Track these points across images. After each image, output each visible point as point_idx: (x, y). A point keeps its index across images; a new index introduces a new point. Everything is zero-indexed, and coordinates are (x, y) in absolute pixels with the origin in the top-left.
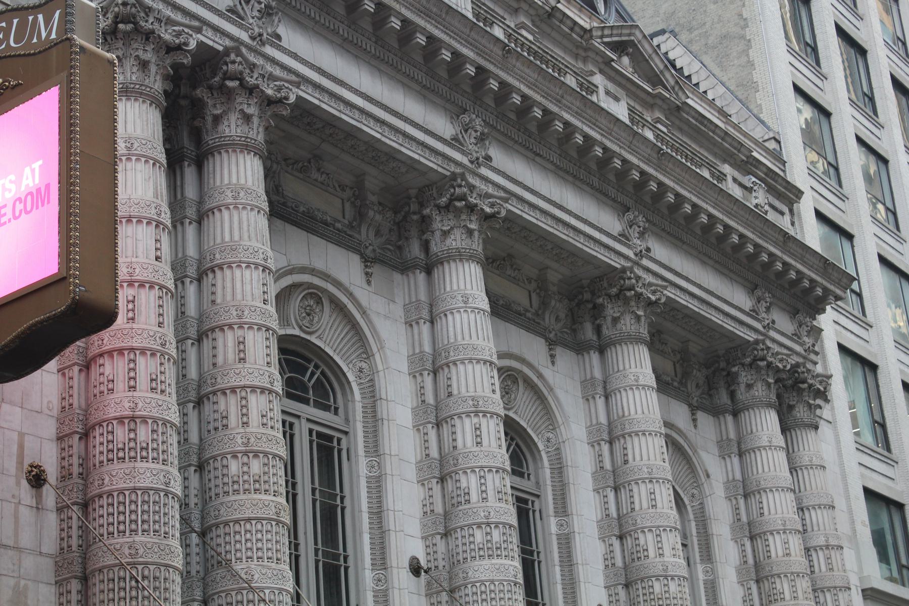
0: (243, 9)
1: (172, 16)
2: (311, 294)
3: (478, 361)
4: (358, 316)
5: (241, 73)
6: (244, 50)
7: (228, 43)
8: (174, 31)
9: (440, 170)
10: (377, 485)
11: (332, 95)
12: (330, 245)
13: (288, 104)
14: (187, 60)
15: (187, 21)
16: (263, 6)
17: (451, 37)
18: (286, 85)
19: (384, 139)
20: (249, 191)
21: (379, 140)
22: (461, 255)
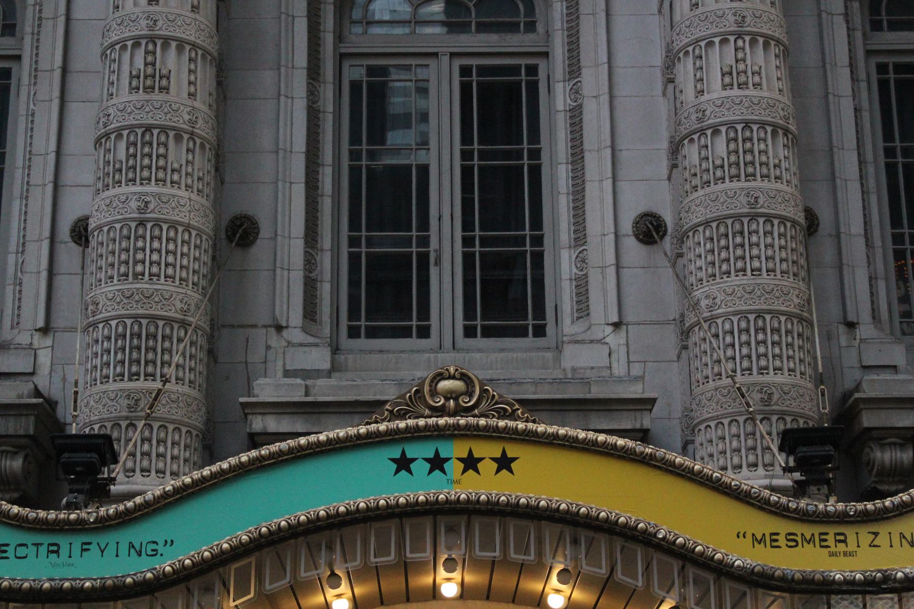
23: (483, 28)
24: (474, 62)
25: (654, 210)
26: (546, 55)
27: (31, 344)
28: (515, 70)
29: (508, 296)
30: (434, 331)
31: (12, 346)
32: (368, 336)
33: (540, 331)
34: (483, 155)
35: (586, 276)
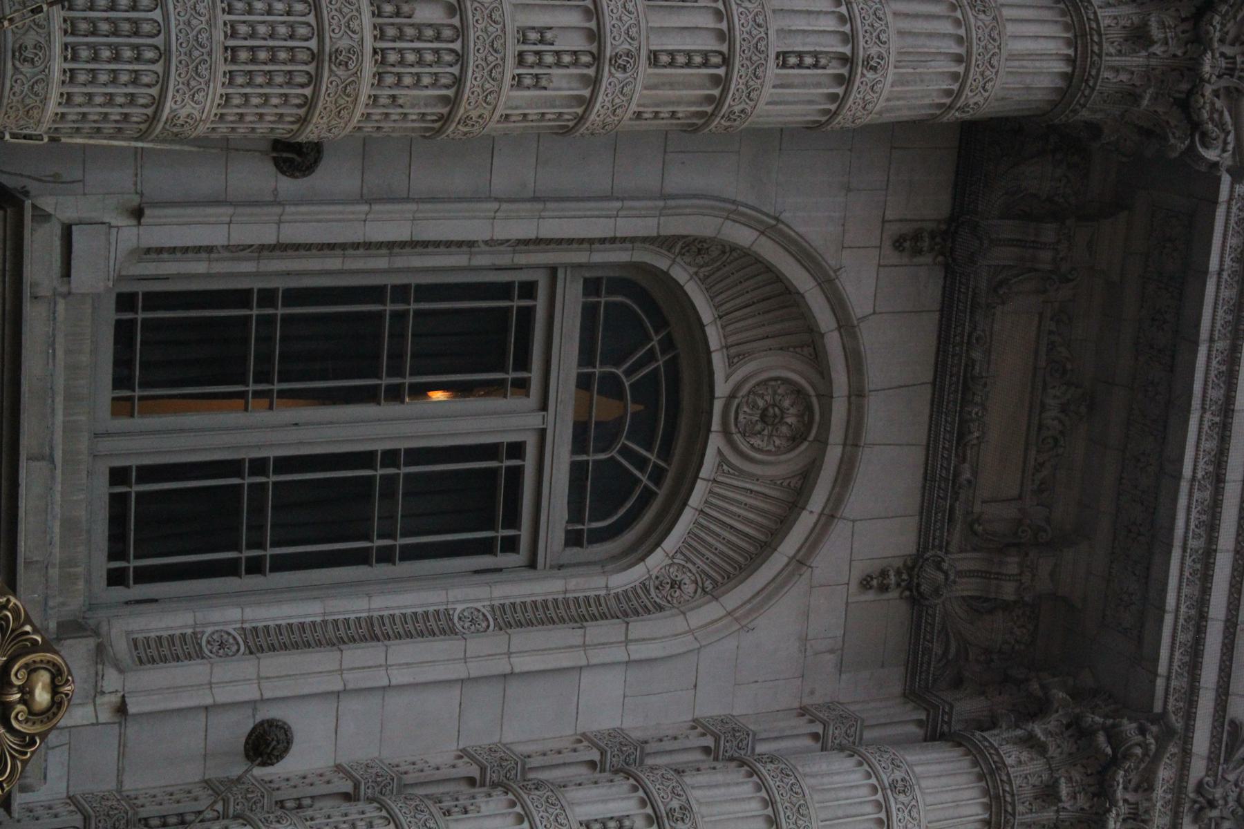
2: (809, 408)
6: (1172, 749)
7: (1178, 724)
8: (1221, 113)
9: (1160, 682)
10: (434, 626)
14: (1178, 145)
19: (1184, 486)
20: (995, 34)
21: (1178, 477)
22: (992, 773)
23: (578, 472)
24: (540, 303)
25: (294, 748)
26: (532, 565)
27: (103, 693)
28: (523, 362)
29: (179, 528)
30: (123, 423)
31: (100, 667)
32: (119, 324)
33: (116, 578)
34: (399, 317)
35: (201, 655)
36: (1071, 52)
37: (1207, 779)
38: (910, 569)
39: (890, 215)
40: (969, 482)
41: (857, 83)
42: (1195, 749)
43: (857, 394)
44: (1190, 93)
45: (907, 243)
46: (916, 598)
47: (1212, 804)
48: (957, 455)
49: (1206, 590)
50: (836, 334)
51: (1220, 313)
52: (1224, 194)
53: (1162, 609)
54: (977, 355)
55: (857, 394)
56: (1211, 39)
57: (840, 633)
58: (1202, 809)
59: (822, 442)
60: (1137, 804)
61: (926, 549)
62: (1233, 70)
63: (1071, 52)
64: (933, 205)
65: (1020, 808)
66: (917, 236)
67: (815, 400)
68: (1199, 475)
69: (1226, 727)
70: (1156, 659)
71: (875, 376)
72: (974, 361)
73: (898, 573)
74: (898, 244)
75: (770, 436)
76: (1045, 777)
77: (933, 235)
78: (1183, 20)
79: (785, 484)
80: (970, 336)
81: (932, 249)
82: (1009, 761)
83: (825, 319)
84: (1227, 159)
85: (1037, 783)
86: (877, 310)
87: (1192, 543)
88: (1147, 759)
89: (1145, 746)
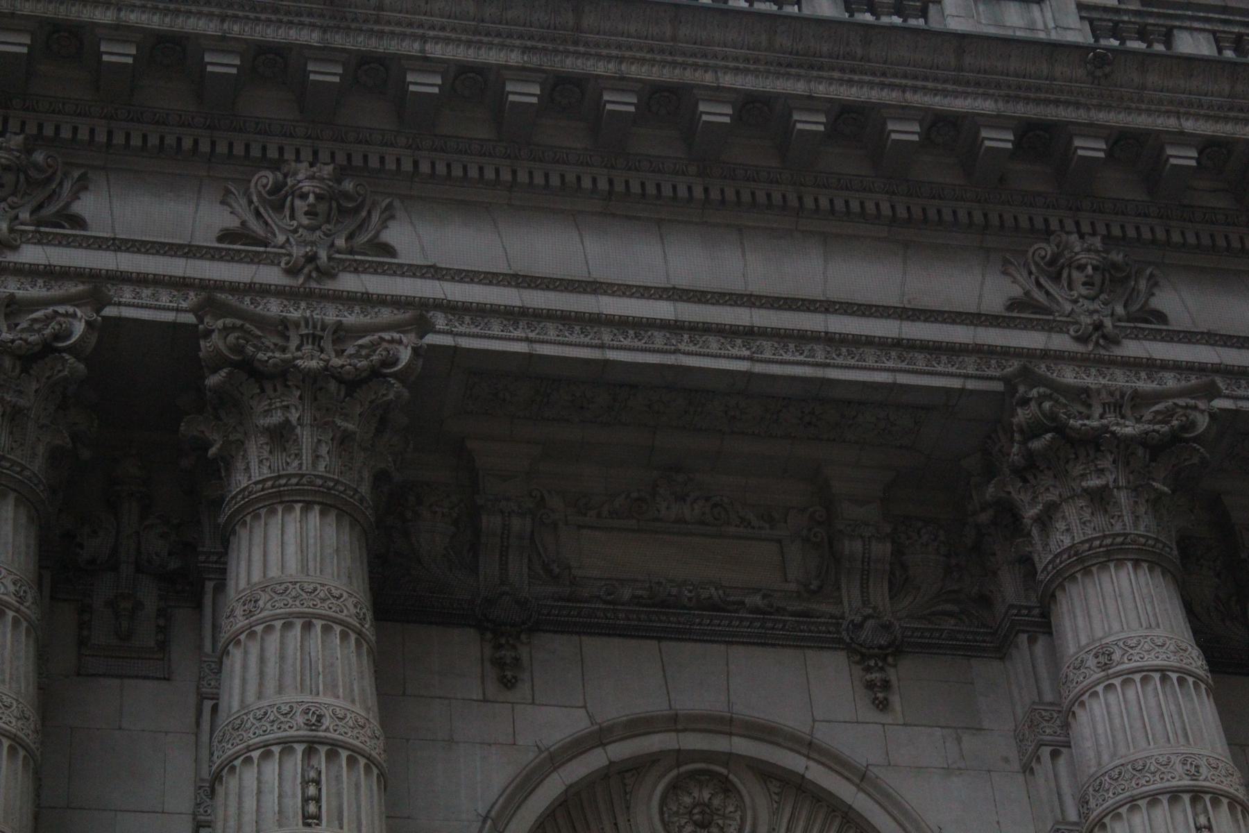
0: (1048, 293)
1: (20, 293)
2: (692, 775)
3: (1153, 799)
4: (845, 791)
5: (1053, 417)
6: (1042, 369)
7: (1014, 366)
8: (361, 346)
9: (971, 385)
11: (566, 319)
12: (739, 653)
13: (1196, 439)
15: (56, 292)
16: (311, 199)
17: (904, 89)
18: (1181, 402)
19: (759, 368)
20: (280, 589)
21: (748, 375)
22: (1081, 560)
36: (298, 507)
37: (1072, 332)
38: (864, 657)
39: (476, 694)
40: (764, 597)
41: (335, 736)
42: (1040, 346)
43: (674, 722)
44: (340, 381)
45: (507, 674)
46: (894, 650)
47: (1098, 326)
48: (736, 611)
49: (869, 341)
50: (610, 748)
51: (573, 339)
52: (447, 341)
53: (893, 387)
54: (626, 593)
55: (674, 722)
56: (283, 361)
57: (938, 732)
58: (1104, 337)
59: (729, 759)
60: (1104, 404)
61: (840, 641)
62: (314, 336)
63: (298, 507)
64: (465, 650)
65: (1118, 528)
66: (499, 664)
67: (683, 769)
68: (747, 353)
69: (1015, 314)
70: (947, 391)
71: (652, 703)
72: (634, 597)
73: (868, 669)
74: (508, 684)
75: (724, 817)
76: (1082, 503)
77: (499, 647)
78: (263, 390)
79: (776, 798)
80: (606, 602)
81: (514, 647)
82: (1067, 542)
83: (595, 760)
84: (409, 339)
85: (1090, 510)
86: (581, 704)
87: (820, 357)
88: (1055, 395)
89: (1041, 398)
